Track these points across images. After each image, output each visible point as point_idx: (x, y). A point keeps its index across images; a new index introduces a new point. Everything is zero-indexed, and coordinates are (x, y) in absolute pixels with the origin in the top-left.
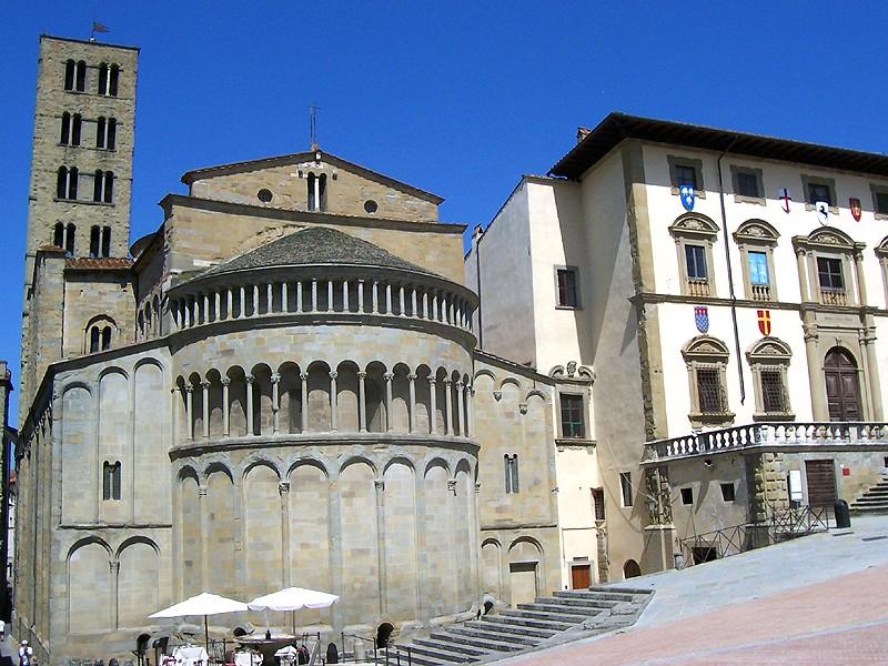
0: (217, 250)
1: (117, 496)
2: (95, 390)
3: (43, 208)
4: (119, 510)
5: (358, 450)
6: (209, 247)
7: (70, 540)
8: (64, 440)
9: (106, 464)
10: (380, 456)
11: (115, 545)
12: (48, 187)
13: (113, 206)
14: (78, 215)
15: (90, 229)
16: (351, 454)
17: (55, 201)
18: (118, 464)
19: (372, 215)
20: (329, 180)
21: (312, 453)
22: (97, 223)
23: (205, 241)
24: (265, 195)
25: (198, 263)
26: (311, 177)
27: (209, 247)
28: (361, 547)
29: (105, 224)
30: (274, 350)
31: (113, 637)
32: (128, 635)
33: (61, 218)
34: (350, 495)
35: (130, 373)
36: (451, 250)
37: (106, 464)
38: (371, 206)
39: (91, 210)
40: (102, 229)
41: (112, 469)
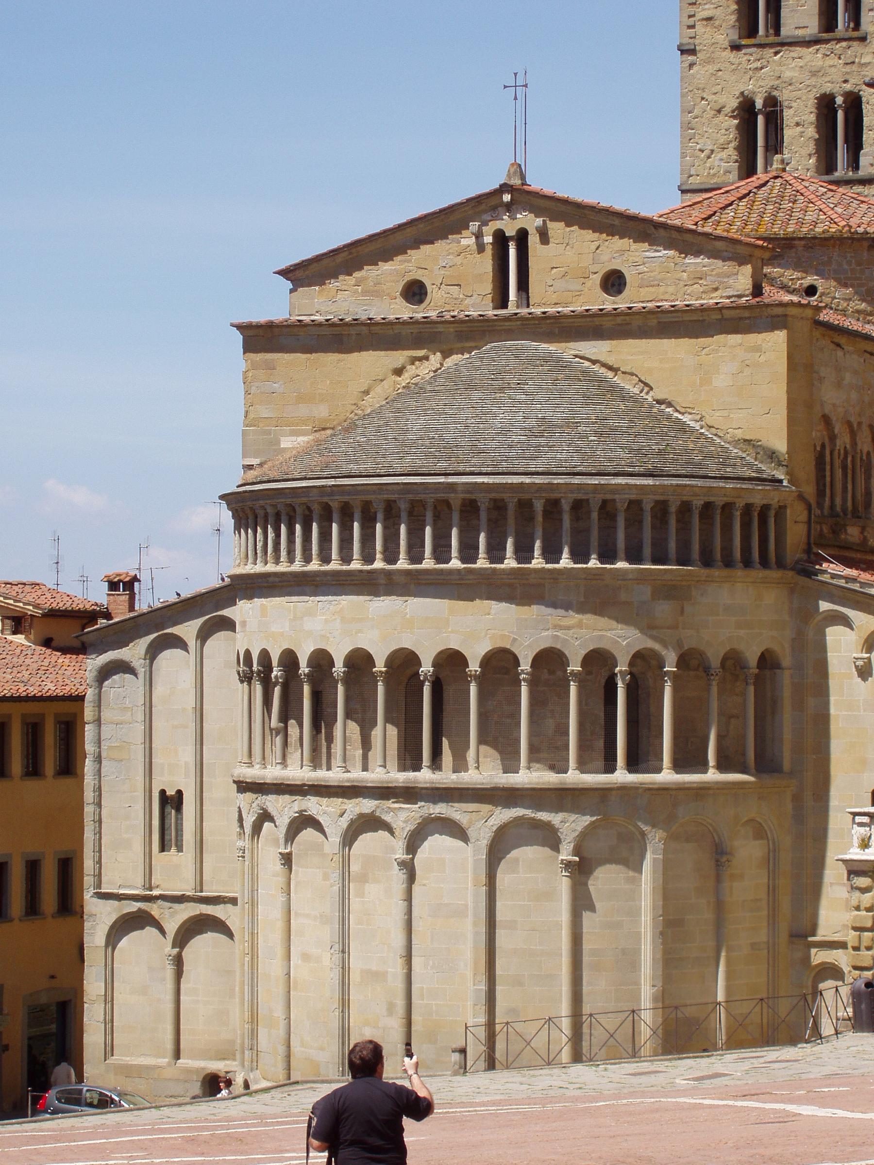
0: (322, 411)
1: (180, 849)
2: (141, 671)
3: (711, 68)
4: (175, 872)
5: (367, 805)
6: (303, 411)
7: (110, 914)
8: (104, 755)
9: (163, 792)
10: (403, 816)
11: (172, 926)
12: (718, 13)
13: (863, 39)
14: (788, 74)
15: (812, 103)
16: (357, 810)
17: (736, 47)
18: (180, 793)
19: (621, 302)
20: (533, 239)
21: (310, 805)
22: (828, 88)
23: (301, 399)
24: (415, 292)
25: (286, 443)
26: (501, 239)
27: (303, 411)
28: (374, 968)
29: (848, 87)
30: (275, 628)
31: (169, 1073)
32: (189, 1071)
33: (749, 87)
34: (364, 879)
35: (192, 643)
36: (763, 359)
37: (163, 792)
38: (614, 282)
39: (812, 57)
40: (839, 100)
41: (172, 802)
